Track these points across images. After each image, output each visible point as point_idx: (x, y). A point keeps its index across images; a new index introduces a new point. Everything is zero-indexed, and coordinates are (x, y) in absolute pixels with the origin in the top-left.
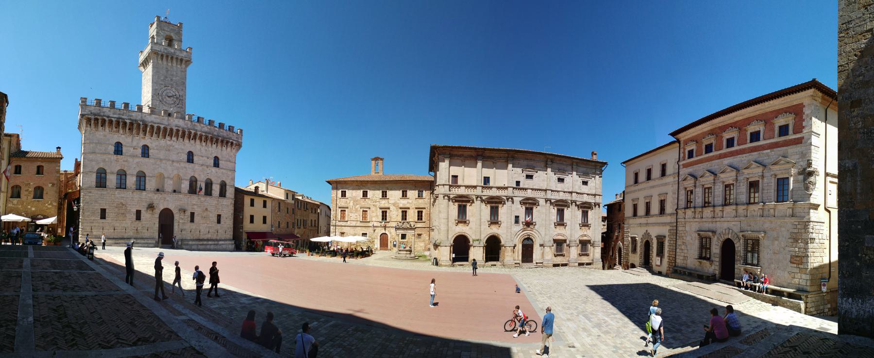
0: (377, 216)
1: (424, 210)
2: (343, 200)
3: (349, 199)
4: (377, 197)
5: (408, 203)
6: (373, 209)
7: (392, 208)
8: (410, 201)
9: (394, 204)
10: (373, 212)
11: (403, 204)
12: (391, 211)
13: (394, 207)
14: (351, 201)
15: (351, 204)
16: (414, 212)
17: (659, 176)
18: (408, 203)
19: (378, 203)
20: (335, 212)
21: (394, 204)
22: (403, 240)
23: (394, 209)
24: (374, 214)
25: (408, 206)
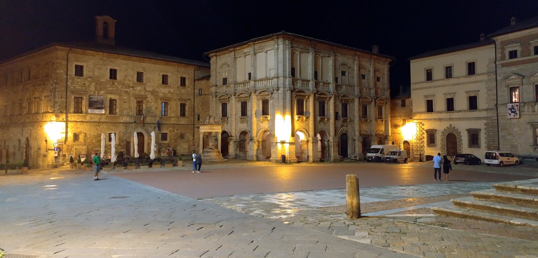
0: (130, 108)
1: (187, 104)
2: (79, 80)
3: (89, 79)
4: (130, 80)
5: (169, 92)
6: (125, 98)
7: (150, 97)
8: (172, 90)
9: (153, 93)
10: (125, 102)
11: (163, 93)
12: (148, 101)
13: (152, 97)
14: (91, 83)
15: (92, 88)
16: (177, 105)
17: (465, 75)
18: (169, 92)
19: (131, 89)
20: (65, 100)
21: (153, 93)
22: (164, 142)
23: (152, 100)
24: (126, 106)
25: (169, 95)
